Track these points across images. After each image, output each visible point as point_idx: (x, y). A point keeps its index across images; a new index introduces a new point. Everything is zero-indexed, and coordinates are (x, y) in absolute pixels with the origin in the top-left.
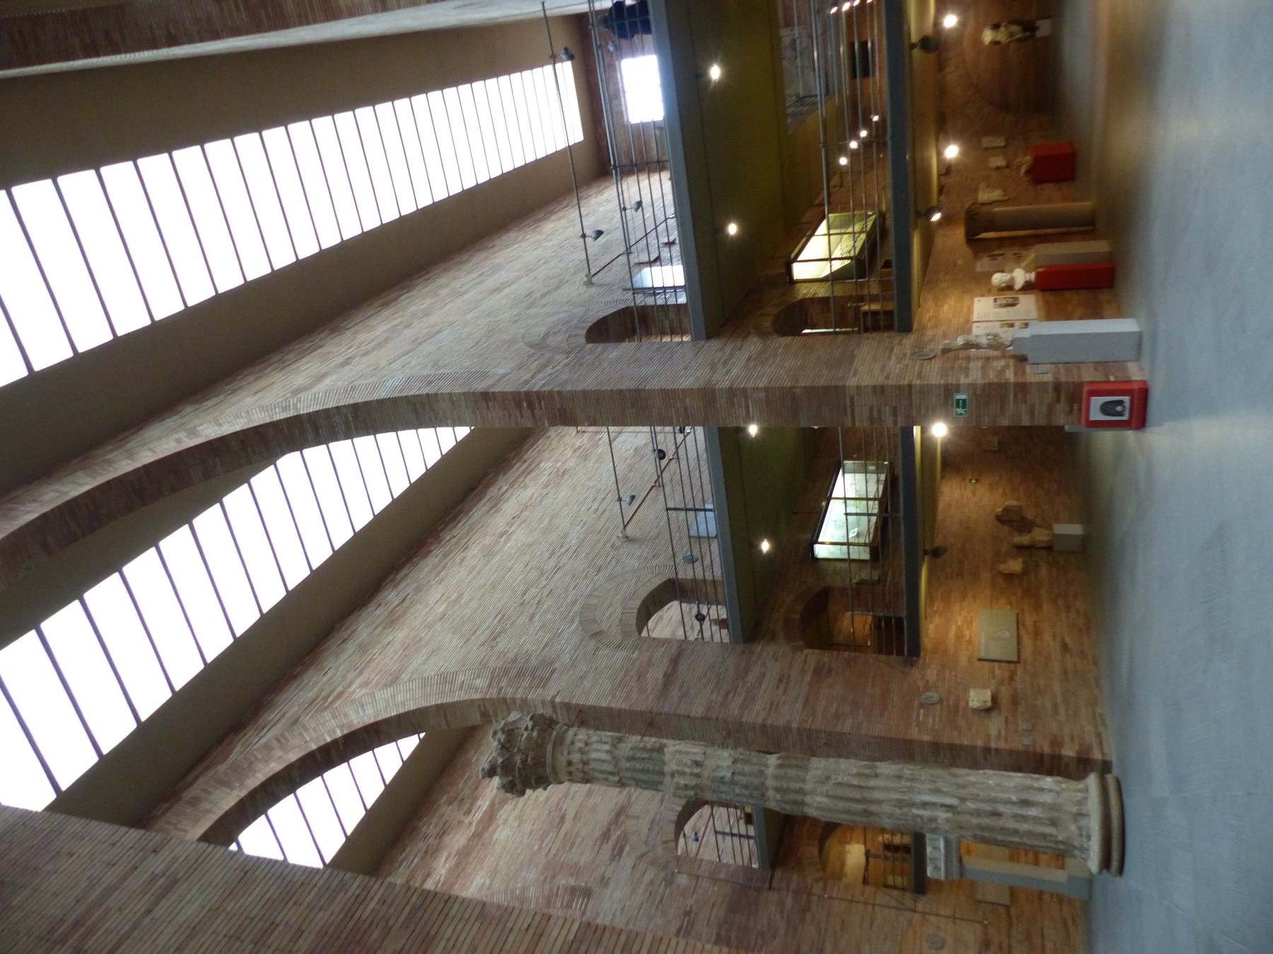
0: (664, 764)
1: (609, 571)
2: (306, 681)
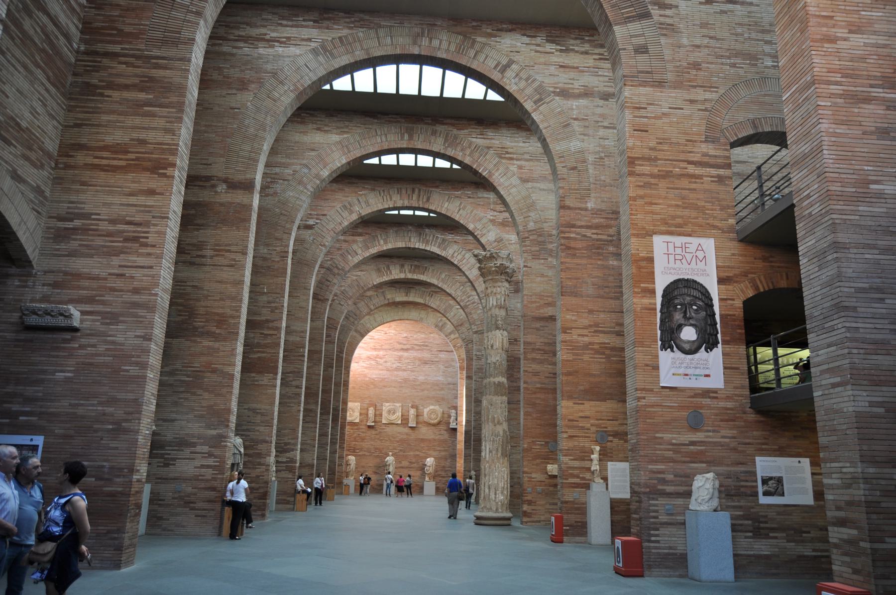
2: (517, 136)
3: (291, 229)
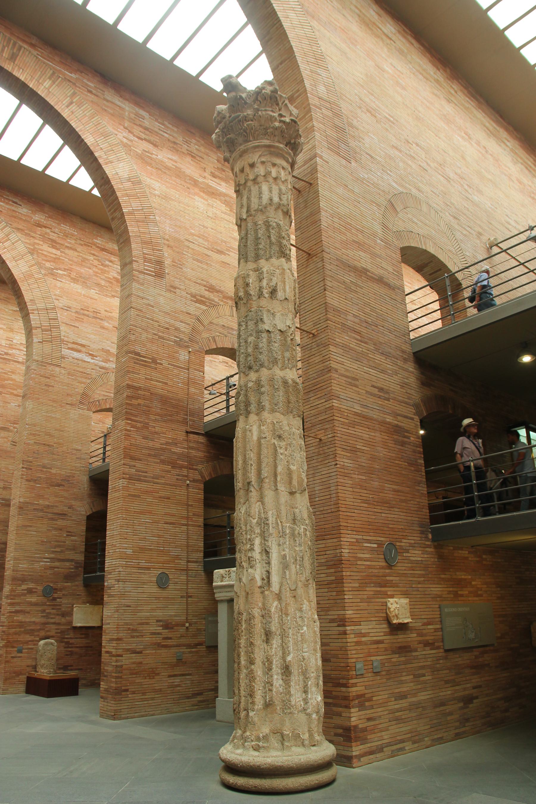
0: (267, 260)
1: (457, 227)
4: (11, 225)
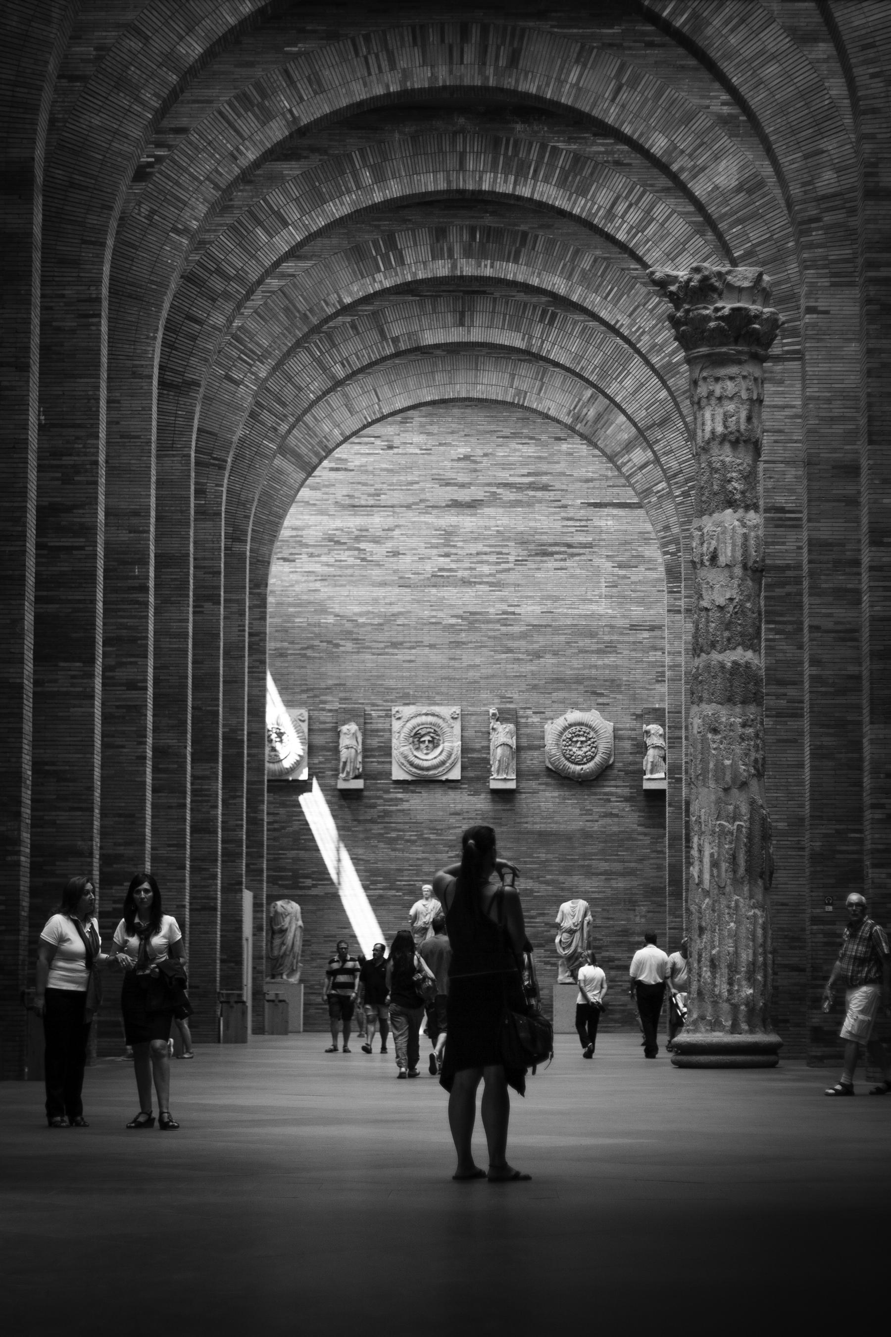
3: (103, 230)
4: (652, 185)
